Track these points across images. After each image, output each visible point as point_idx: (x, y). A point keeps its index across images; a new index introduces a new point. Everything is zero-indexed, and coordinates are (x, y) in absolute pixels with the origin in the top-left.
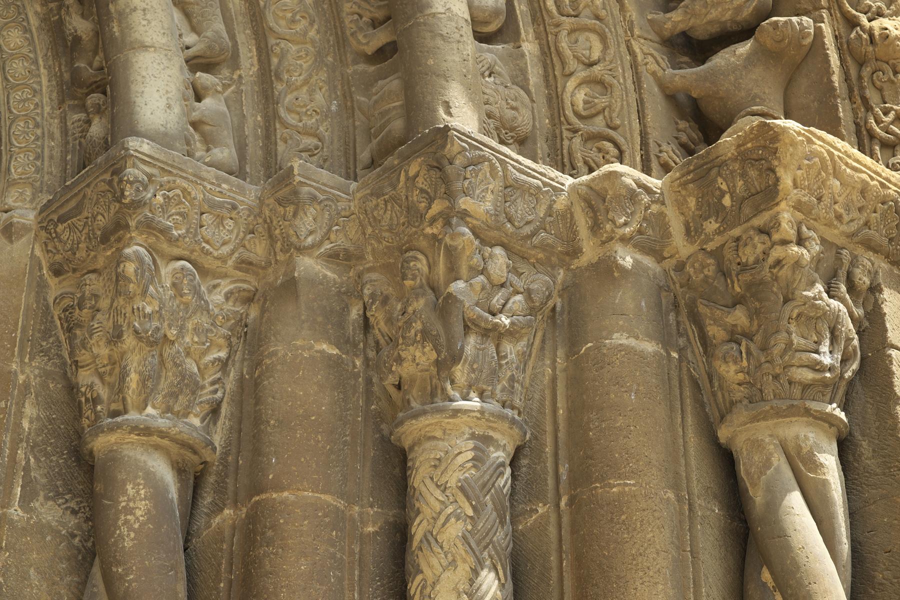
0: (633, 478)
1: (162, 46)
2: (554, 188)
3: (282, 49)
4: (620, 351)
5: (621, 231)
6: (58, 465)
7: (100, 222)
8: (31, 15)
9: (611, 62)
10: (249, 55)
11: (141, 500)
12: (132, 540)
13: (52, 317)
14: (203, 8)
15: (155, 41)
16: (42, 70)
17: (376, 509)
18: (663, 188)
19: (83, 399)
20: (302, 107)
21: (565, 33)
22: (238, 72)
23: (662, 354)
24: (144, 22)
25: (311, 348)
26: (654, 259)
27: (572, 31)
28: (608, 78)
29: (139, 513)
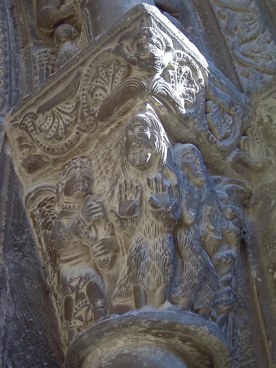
7: (99, 97)
13: (24, 214)
19: (73, 296)
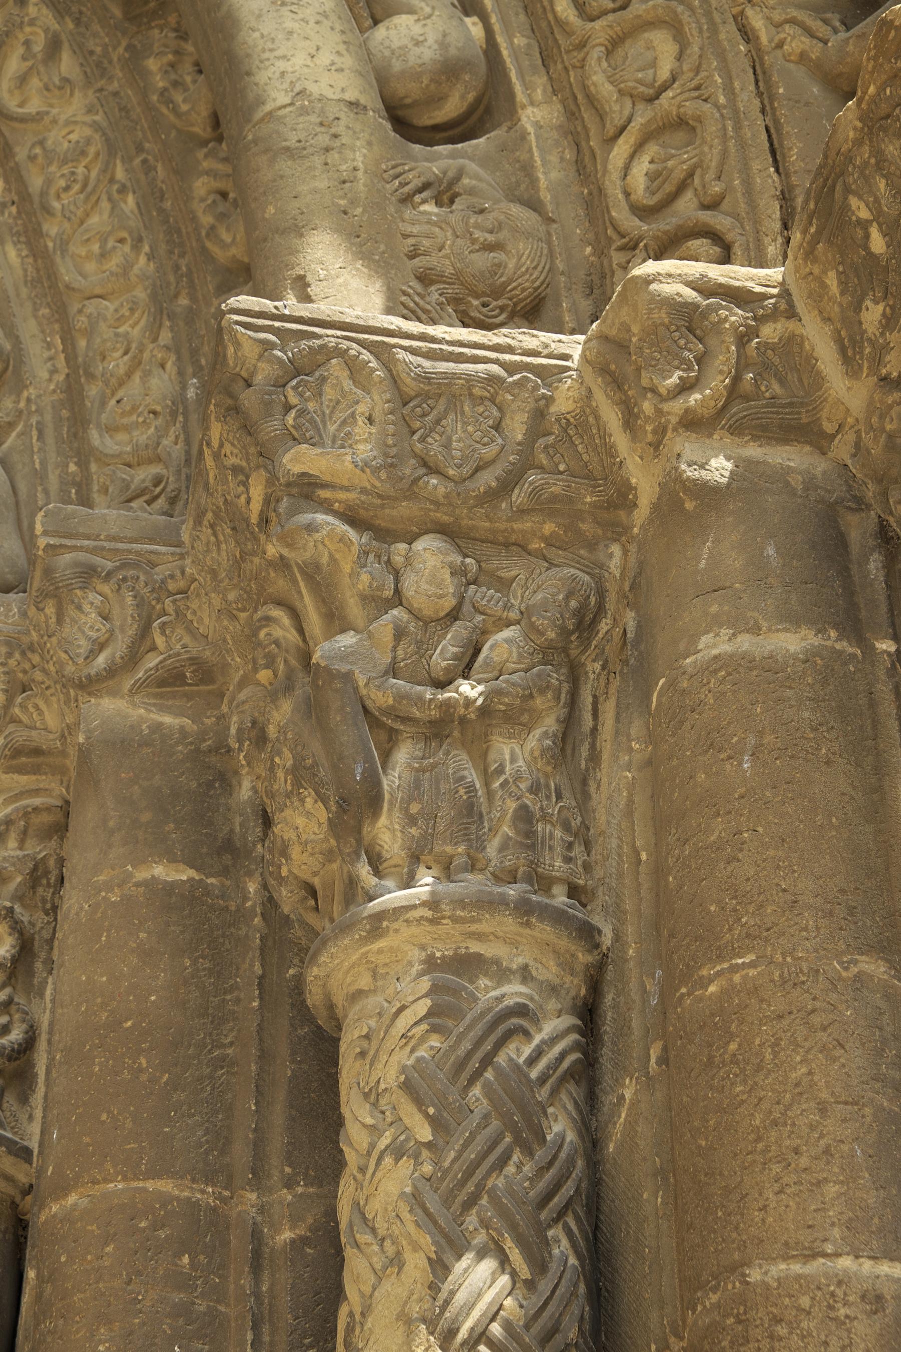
0: (750, 950)
2: (539, 371)
4: (716, 671)
5: (676, 407)
9: (697, 71)
10: (46, 354)
17: (300, 1190)
18: (788, 281)
20: (130, 413)
21: (597, 52)
23: (840, 653)
26: (807, 448)
27: (614, 44)
28: (690, 108)
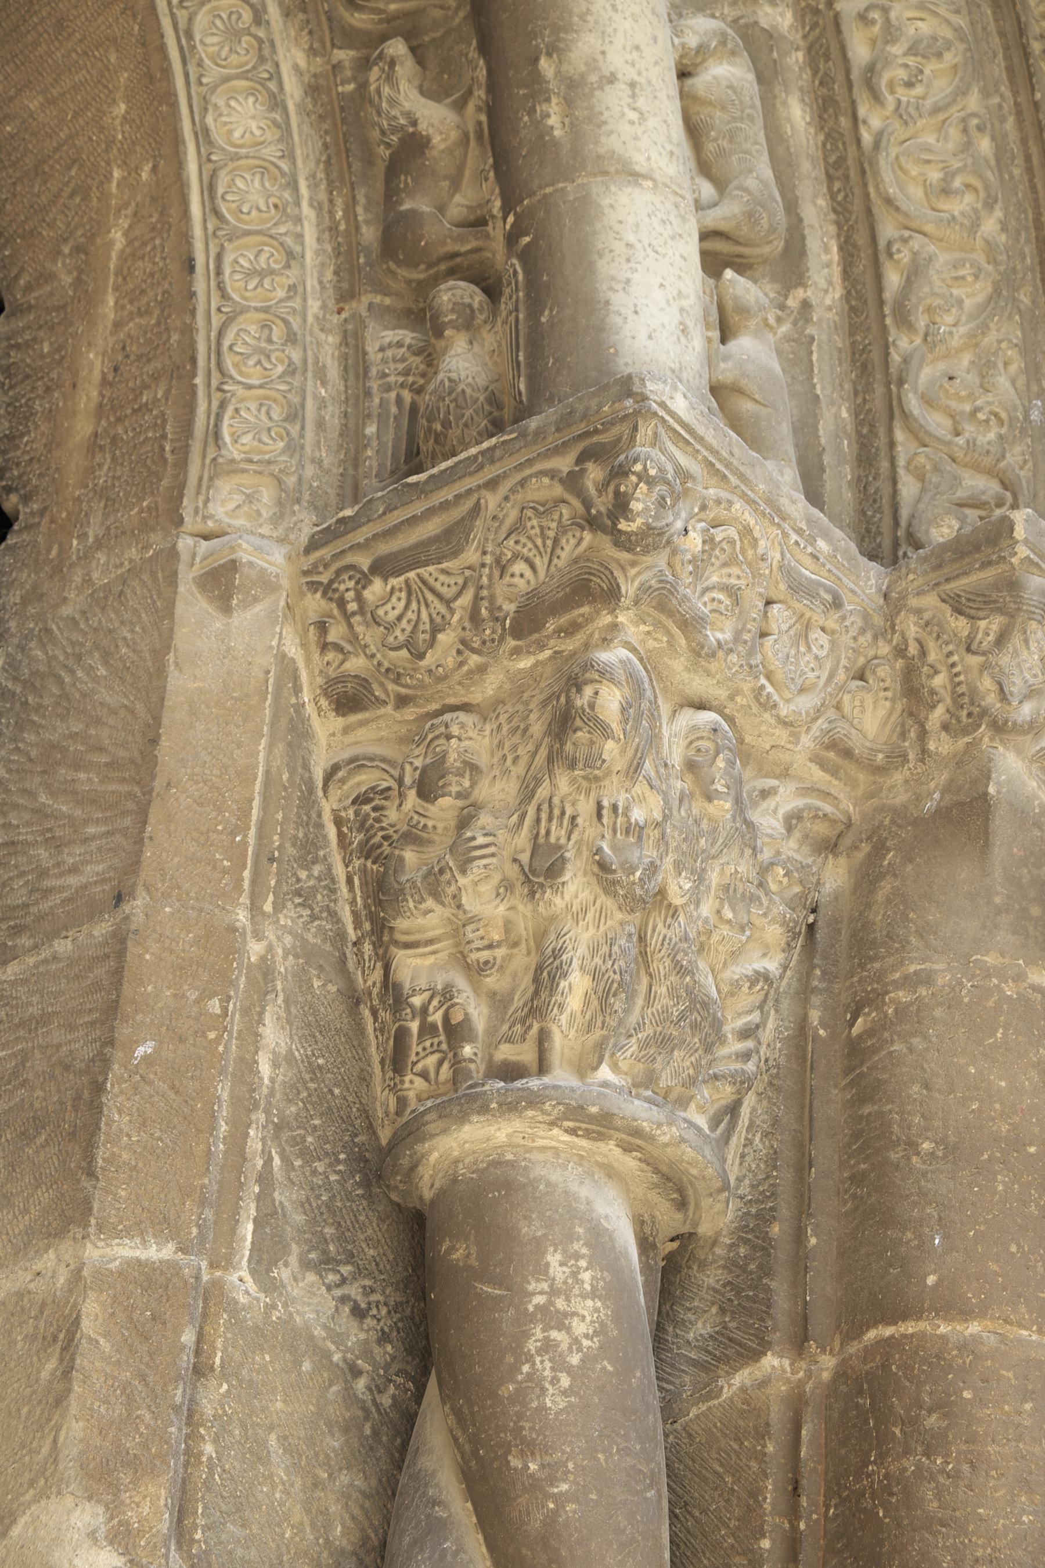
1: (668, 181)
3: (915, 254)
6: (328, 1186)
7: (517, 580)
8: (285, 69)
10: (825, 258)
11: (584, 1296)
12: (564, 1393)
13: (319, 816)
14: (735, 119)
15: (654, 165)
16: (306, 210)
19: (414, 1026)
20: (961, 399)
22: (800, 293)
24: (633, 116)
25: (1019, 977)
29: (580, 1328)
